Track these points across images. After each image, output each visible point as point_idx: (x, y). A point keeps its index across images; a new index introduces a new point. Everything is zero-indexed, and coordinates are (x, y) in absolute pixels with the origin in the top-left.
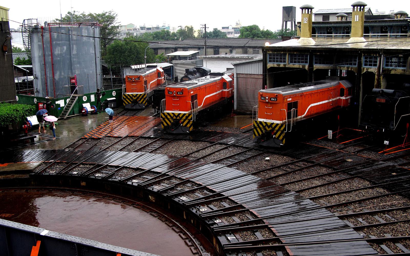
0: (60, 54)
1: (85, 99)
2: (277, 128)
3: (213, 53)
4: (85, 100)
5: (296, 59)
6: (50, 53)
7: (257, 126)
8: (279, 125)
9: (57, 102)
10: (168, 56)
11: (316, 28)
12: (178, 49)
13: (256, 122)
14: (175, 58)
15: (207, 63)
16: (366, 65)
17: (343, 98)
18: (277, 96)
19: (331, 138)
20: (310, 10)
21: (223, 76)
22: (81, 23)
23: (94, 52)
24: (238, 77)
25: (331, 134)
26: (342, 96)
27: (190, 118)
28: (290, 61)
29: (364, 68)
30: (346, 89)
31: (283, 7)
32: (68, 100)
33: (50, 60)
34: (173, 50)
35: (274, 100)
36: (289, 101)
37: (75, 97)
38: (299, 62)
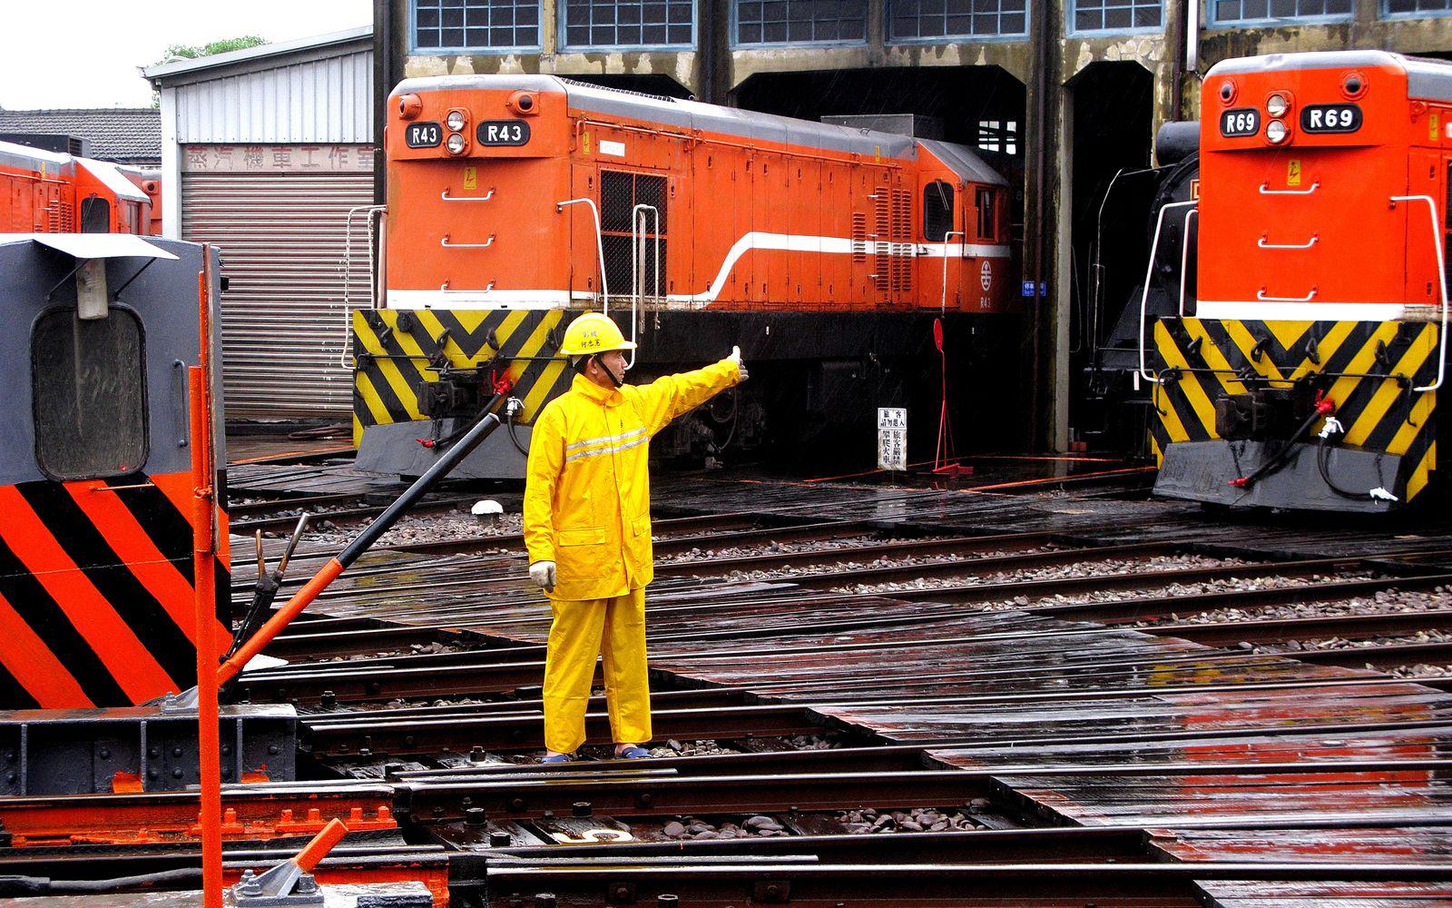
2: (531, 348)
7: (383, 352)
8: (550, 322)
13: (374, 320)
16: (1085, 21)
17: (946, 250)
18: (526, 104)
19: (902, 467)
24: (193, 168)
25: (896, 435)
26: (936, 238)
28: (564, 33)
29: (1074, 46)
30: (962, 189)
35: (505, 135)
36: (612, 160)
38: (628, 36)
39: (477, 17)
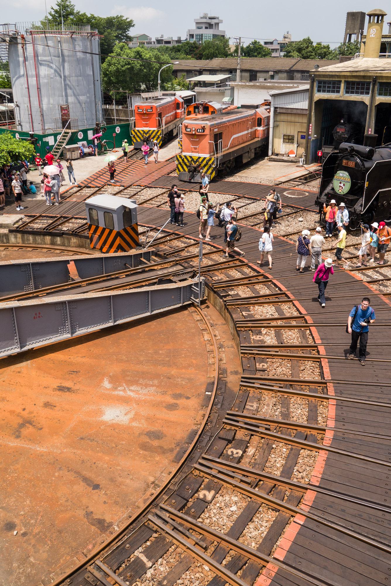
0: (48, 75)
1: (80, 136)
3: (248, 79)
4: (80, 138)
5: (353, 88)
6: (34, 73)
9: (45, 140)
10: (190, 81)
11: (388, 44)
12: (203, 73)
14: (199, 84)
15: (240, 92)
20: (380, 17)
21: (257, 110)
22: (73, 32)
23: (92, 74)
27: (210, 163)
31: (348, 13)
32: (59, 137)
33: (35, 83)
34: (197, 73)
37: (68, 133)
39: (329, 87)
